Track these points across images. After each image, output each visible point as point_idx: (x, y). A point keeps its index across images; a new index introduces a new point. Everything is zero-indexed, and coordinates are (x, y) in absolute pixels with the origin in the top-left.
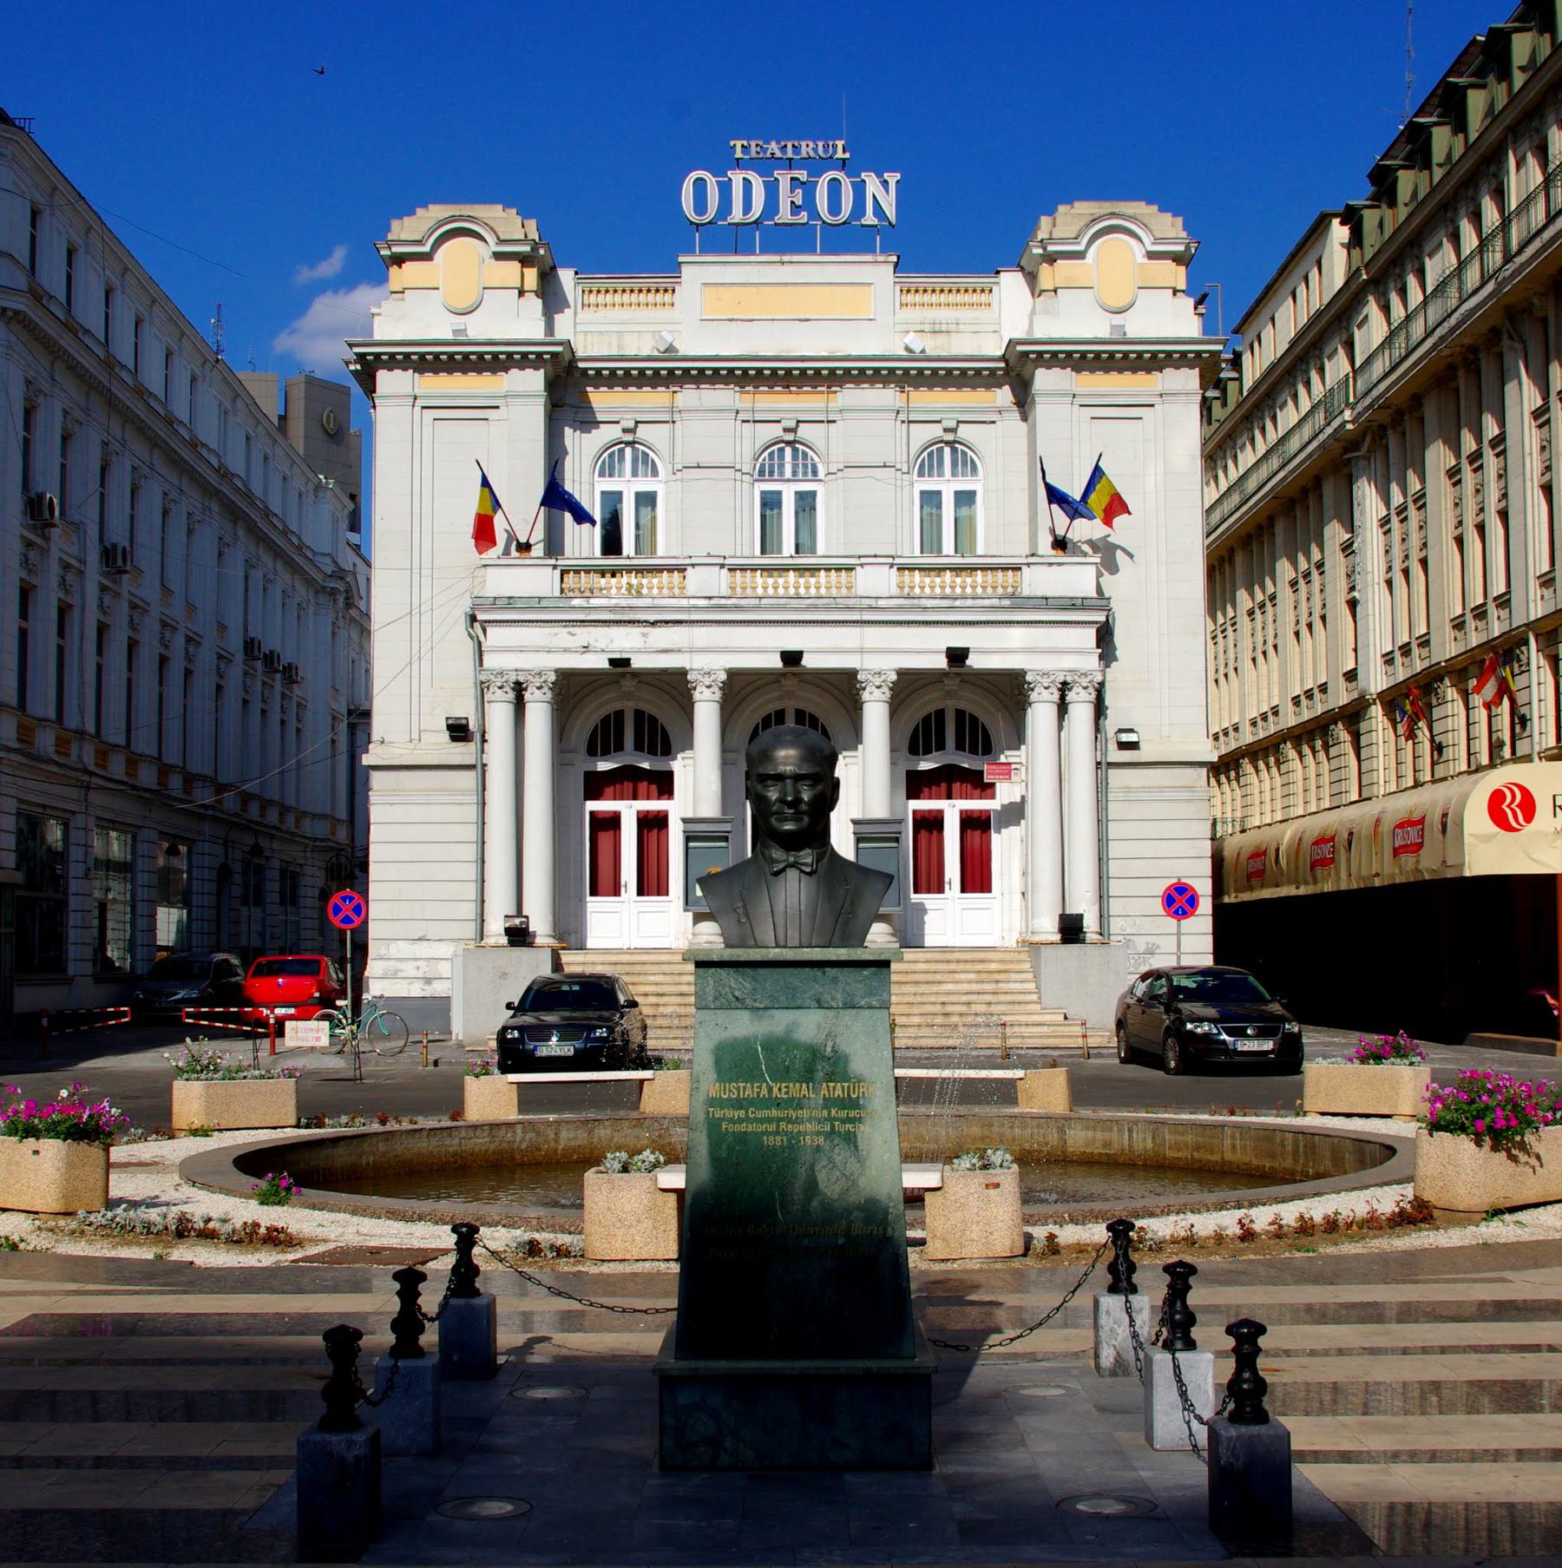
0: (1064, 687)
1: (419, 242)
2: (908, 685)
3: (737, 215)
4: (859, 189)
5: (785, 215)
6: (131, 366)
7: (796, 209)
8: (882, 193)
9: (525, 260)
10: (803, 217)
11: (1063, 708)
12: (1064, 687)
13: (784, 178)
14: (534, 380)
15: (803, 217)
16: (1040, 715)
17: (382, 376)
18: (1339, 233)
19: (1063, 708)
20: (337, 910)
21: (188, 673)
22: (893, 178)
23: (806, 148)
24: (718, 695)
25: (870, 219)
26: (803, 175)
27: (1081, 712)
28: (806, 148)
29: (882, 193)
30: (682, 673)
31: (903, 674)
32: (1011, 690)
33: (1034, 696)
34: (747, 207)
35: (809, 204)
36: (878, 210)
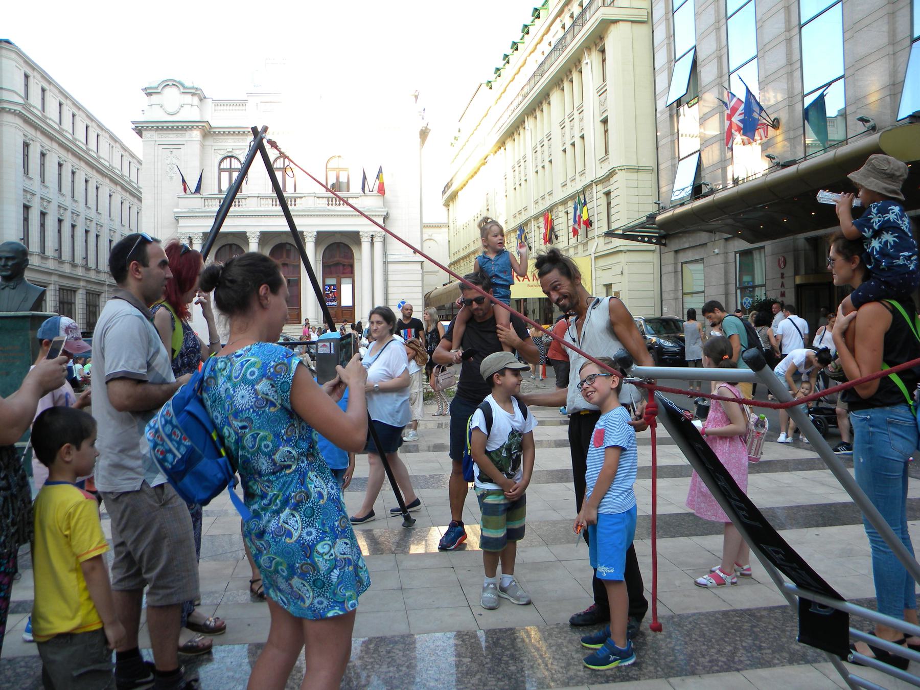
0: (372, 237)
1: (157, 88)
2: (321, 236)
6: (71, 132)
9: (193, 94)
11: (372, 243)
12: (372, 237)
14: (196, 134)
16: (366, 245)
17: (144, 133)
18: (485, 88)
19: (372, 243)
21: (97, 236)
24: (257, 240)
27: (378, 246)
30: (245, 233)
31: (319, 233)
32: (355, 237)
33: (362, 240)
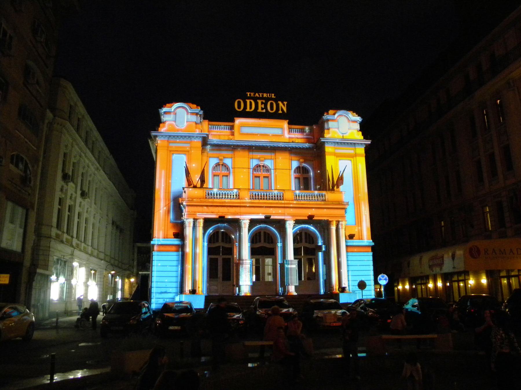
3: (248, 110)
4: (278, 106)
5: (260, 110)
7: (262, 109)
8: (283, 106)
10: (264, 111)
13: (260, 102)
15: (264, 111)
22: (285, 103)
23: (265, 95)
25: (280, 112)
26: (264, 101)
28: (265, 95)
29: (283, 106)
34: (251, 108)
35: (266, 107)
36: (282, 110)
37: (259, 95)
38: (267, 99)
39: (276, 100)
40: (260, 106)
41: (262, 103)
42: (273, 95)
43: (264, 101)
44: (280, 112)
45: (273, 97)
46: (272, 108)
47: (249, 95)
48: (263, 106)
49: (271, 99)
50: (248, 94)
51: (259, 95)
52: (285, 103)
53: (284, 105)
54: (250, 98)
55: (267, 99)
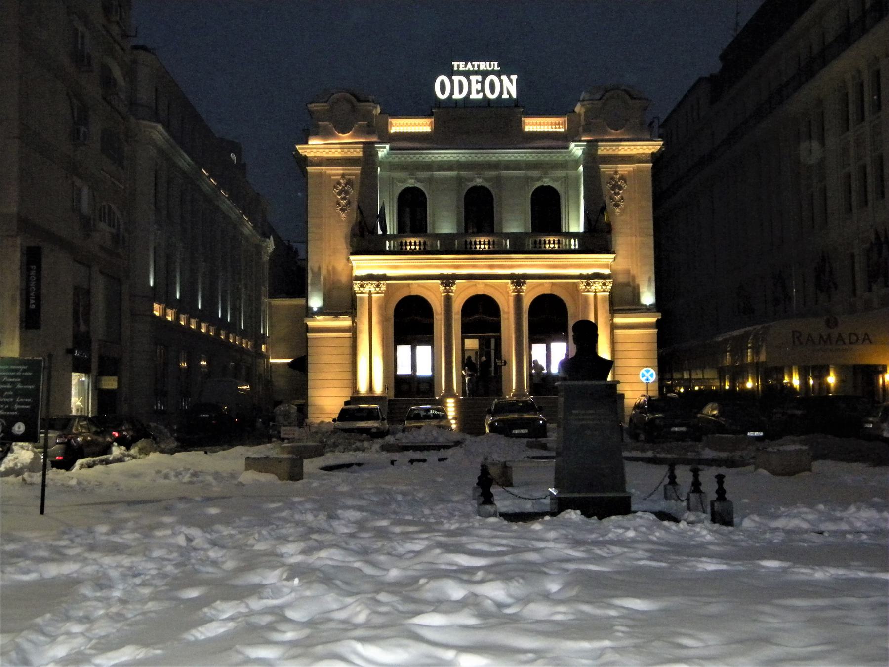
20: (648, 371)
37: (473, 66)
38: (485, 74)
39: (498, 74)
40: (476, 87)
41: (477, 82)
42: (496, 63)
43: (479, 78)
44: (505, 96)
45: (496, 68)
46: (493, 90)
47: (456, 68)
48: (479, 86)
49: (493, 72)
50: (455, 64)
51: (473, 66)
52: (514, 77)
53: (511, 81)
54: (459, 73)
55: (485, 74)
